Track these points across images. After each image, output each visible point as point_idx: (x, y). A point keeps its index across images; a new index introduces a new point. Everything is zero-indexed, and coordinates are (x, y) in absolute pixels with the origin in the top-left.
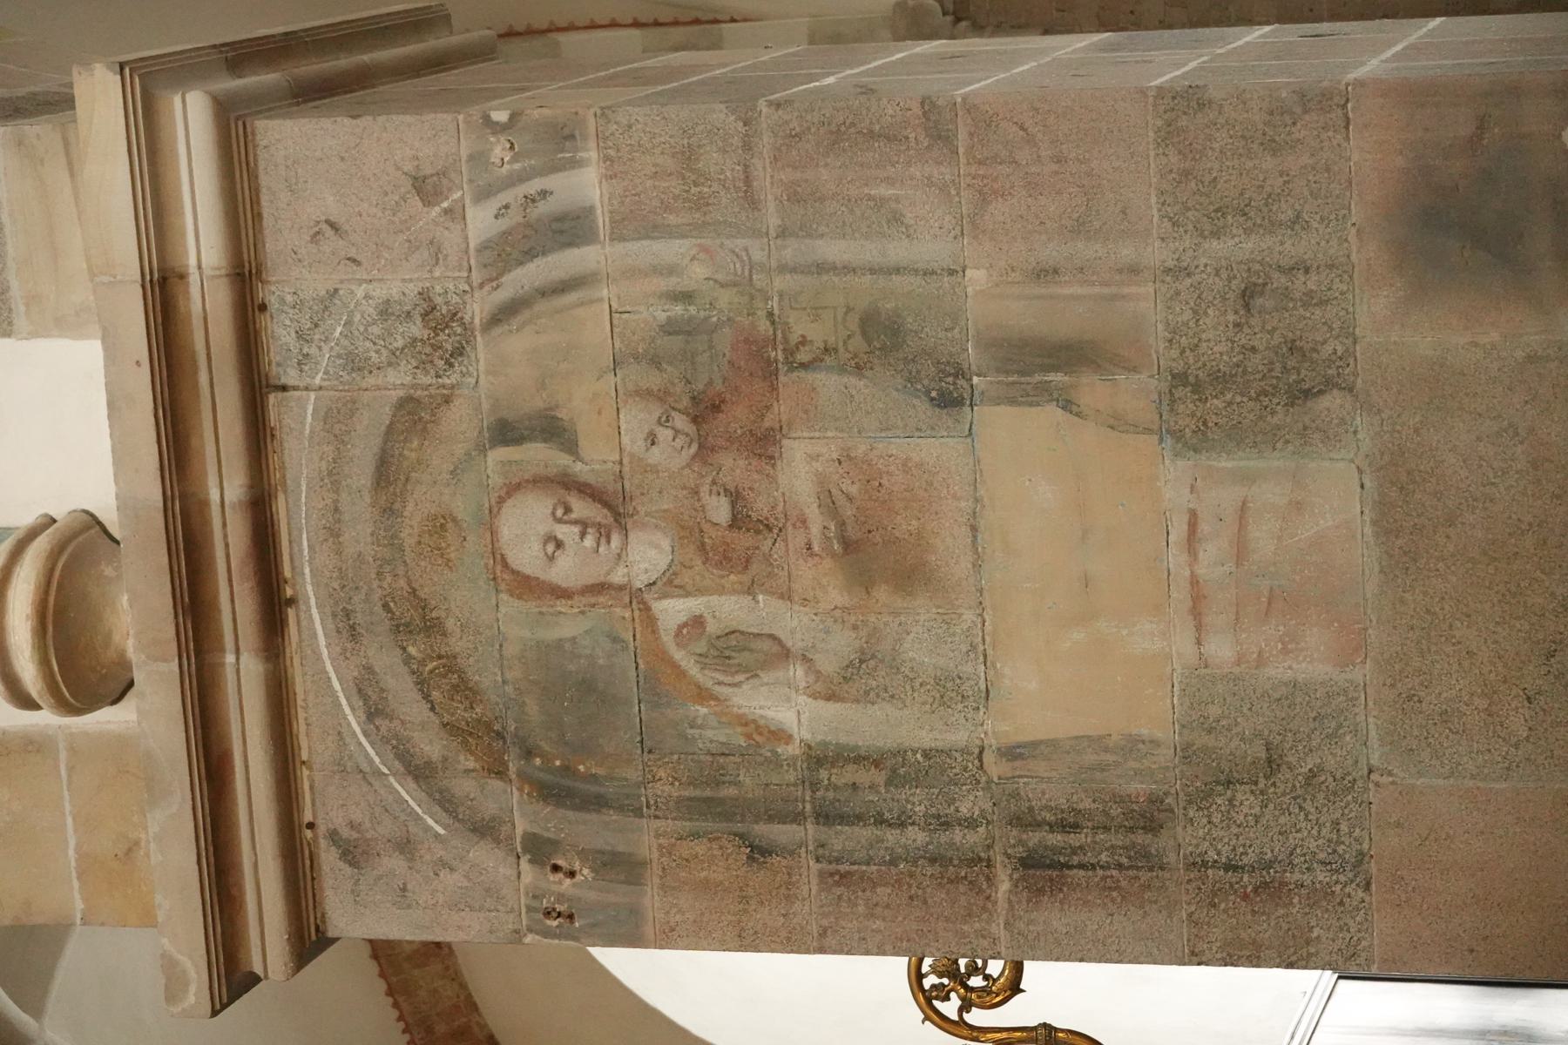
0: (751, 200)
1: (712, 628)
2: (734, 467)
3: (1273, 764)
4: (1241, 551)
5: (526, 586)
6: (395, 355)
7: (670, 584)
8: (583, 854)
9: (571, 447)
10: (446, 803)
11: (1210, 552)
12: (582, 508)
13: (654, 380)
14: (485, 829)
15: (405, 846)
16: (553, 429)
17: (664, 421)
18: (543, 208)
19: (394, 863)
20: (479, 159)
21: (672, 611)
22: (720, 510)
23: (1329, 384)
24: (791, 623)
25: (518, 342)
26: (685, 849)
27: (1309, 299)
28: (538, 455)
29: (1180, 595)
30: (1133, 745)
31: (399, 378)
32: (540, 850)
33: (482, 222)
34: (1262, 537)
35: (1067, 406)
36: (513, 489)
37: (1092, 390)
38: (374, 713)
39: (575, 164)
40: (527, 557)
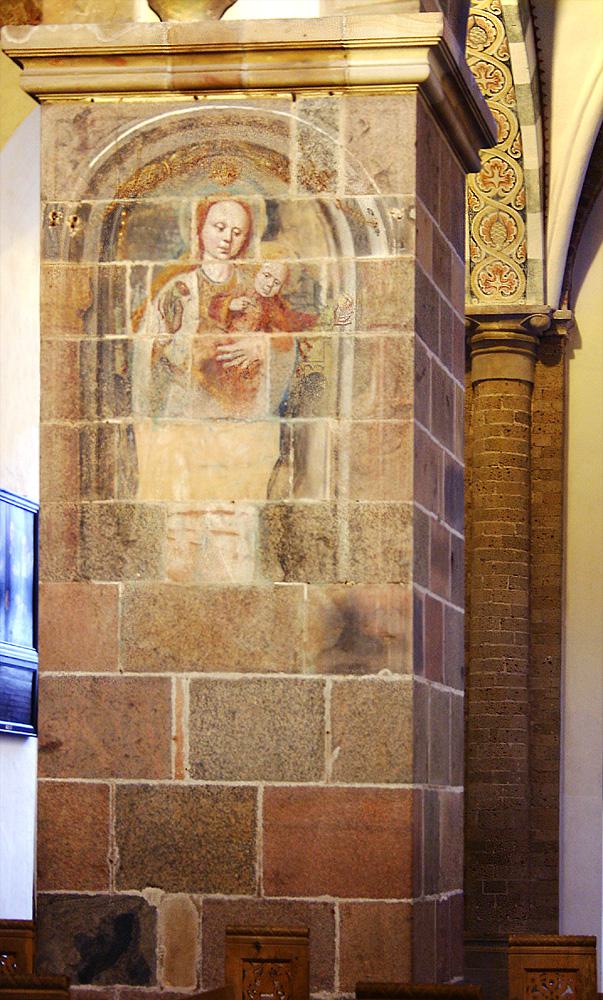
0: (372, 327)
1: (184, 299)
2: (256, 312)
3: (127, 543)
4: (217, 533)
5: (203, 213)
6: (307, 157)
7: (204, 281)
8: (82, 233)
9: (264, 238)
10: (104, 168)
11: (216, 519)
12: (238, 241)
13: (294, 278)
14: (93, 187)
15: (84, 147)
16: (273, 231)
17: (276, 282)
18: (371, 231)
19: (76, 142)
20: (395, 202)
21: (191, 281)
22: (236, 305)
23: (287, 572)
24: (188, 334)
25: (313, 216)
26: (86, 281)
27: (322, 565)
28: (261, 222)
29: (199, 506)
30: (134, 485)
31: (295, 156)
32: (84, 212)
33: (366, 202)
34: (221, 542)
35: (279, 462)
36: (247, 208)
37: (288, 476)
38: (146, 136)
39: (391, 251)
40: (215, 214)
